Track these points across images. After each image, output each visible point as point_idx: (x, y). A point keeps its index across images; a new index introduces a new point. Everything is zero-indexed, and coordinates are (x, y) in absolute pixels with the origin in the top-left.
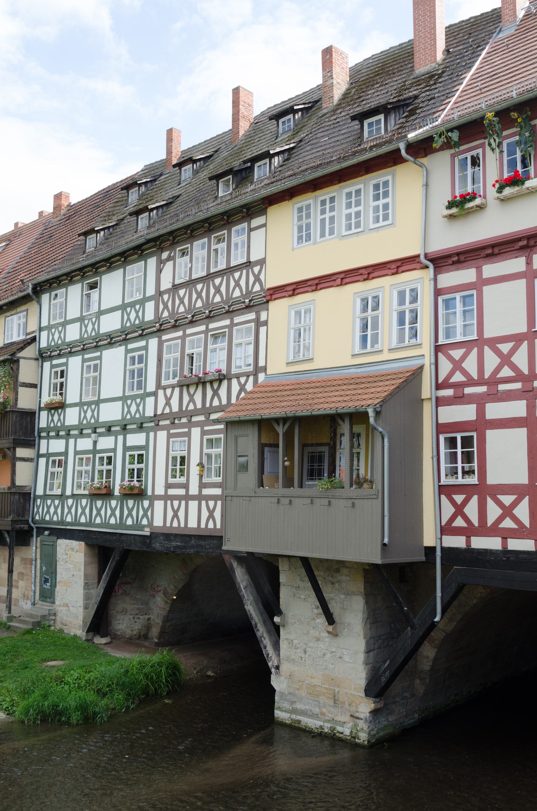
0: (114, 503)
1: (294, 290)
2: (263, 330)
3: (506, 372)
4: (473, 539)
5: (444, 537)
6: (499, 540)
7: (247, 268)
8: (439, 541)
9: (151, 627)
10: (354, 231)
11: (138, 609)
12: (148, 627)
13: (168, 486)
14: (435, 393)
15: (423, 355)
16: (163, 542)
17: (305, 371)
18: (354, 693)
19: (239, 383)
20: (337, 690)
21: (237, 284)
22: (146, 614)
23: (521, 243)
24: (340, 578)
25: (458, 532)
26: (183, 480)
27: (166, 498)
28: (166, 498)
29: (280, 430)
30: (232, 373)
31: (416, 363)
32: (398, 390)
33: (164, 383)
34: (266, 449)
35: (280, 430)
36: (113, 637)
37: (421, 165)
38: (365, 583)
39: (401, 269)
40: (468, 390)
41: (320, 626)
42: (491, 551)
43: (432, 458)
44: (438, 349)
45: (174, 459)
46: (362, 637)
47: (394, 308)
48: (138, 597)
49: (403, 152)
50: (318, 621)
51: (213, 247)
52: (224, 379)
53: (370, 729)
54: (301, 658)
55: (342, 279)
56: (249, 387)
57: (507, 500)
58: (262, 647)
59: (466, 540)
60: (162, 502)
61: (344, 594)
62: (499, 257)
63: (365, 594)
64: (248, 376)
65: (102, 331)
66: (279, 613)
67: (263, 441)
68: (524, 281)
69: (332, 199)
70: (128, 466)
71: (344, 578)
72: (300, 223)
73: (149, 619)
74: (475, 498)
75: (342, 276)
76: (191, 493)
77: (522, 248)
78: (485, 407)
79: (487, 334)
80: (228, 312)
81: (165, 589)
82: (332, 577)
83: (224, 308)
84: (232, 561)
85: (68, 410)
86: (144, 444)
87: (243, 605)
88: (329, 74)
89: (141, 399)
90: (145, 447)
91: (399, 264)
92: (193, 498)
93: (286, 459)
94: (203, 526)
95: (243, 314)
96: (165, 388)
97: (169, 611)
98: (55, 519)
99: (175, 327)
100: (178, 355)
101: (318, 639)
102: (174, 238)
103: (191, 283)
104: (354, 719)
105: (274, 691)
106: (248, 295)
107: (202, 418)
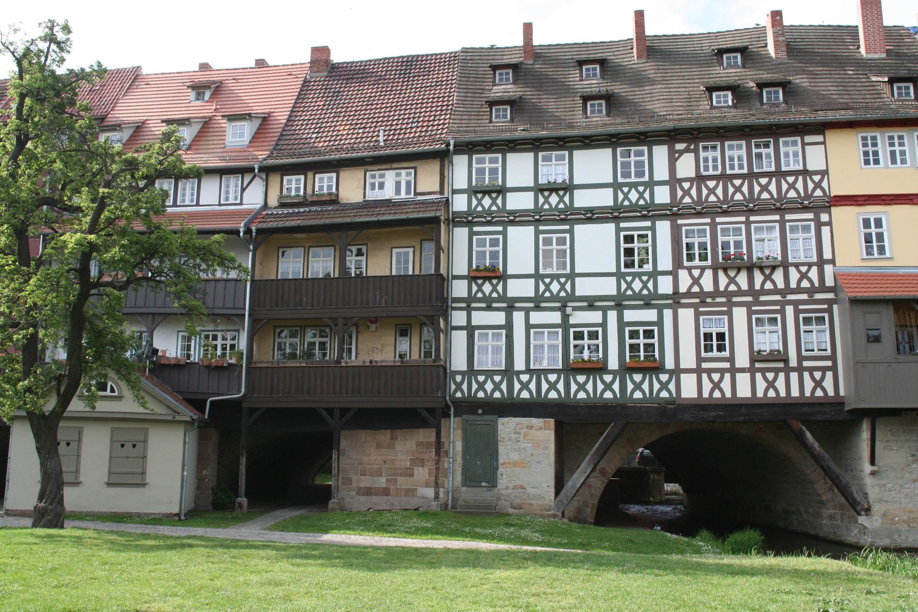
0: (608, 378)
2: (825, 230)
13: (700, 360)
19: (799, 271)
21: (792, 186)
26: (726, 354)
27: (698, 371)
33: (686, 263)
45: (708, 336)
50: (914, 466)
51: (754, 151)
52: (779, 266)
56: (814, 274)
60: (694, 376)
65: (577, 204)
69: (901, 138)
70: (628, 341)
76: (737, 366)
85: (509, 281)
90: (660, 323)
92: (742, 370)
94: (760, 394)
96: (689, 269)
98: (497, 395)
99: (699, 214)
100: (708, 240)
103: (725, 178)
107: (750, 299)
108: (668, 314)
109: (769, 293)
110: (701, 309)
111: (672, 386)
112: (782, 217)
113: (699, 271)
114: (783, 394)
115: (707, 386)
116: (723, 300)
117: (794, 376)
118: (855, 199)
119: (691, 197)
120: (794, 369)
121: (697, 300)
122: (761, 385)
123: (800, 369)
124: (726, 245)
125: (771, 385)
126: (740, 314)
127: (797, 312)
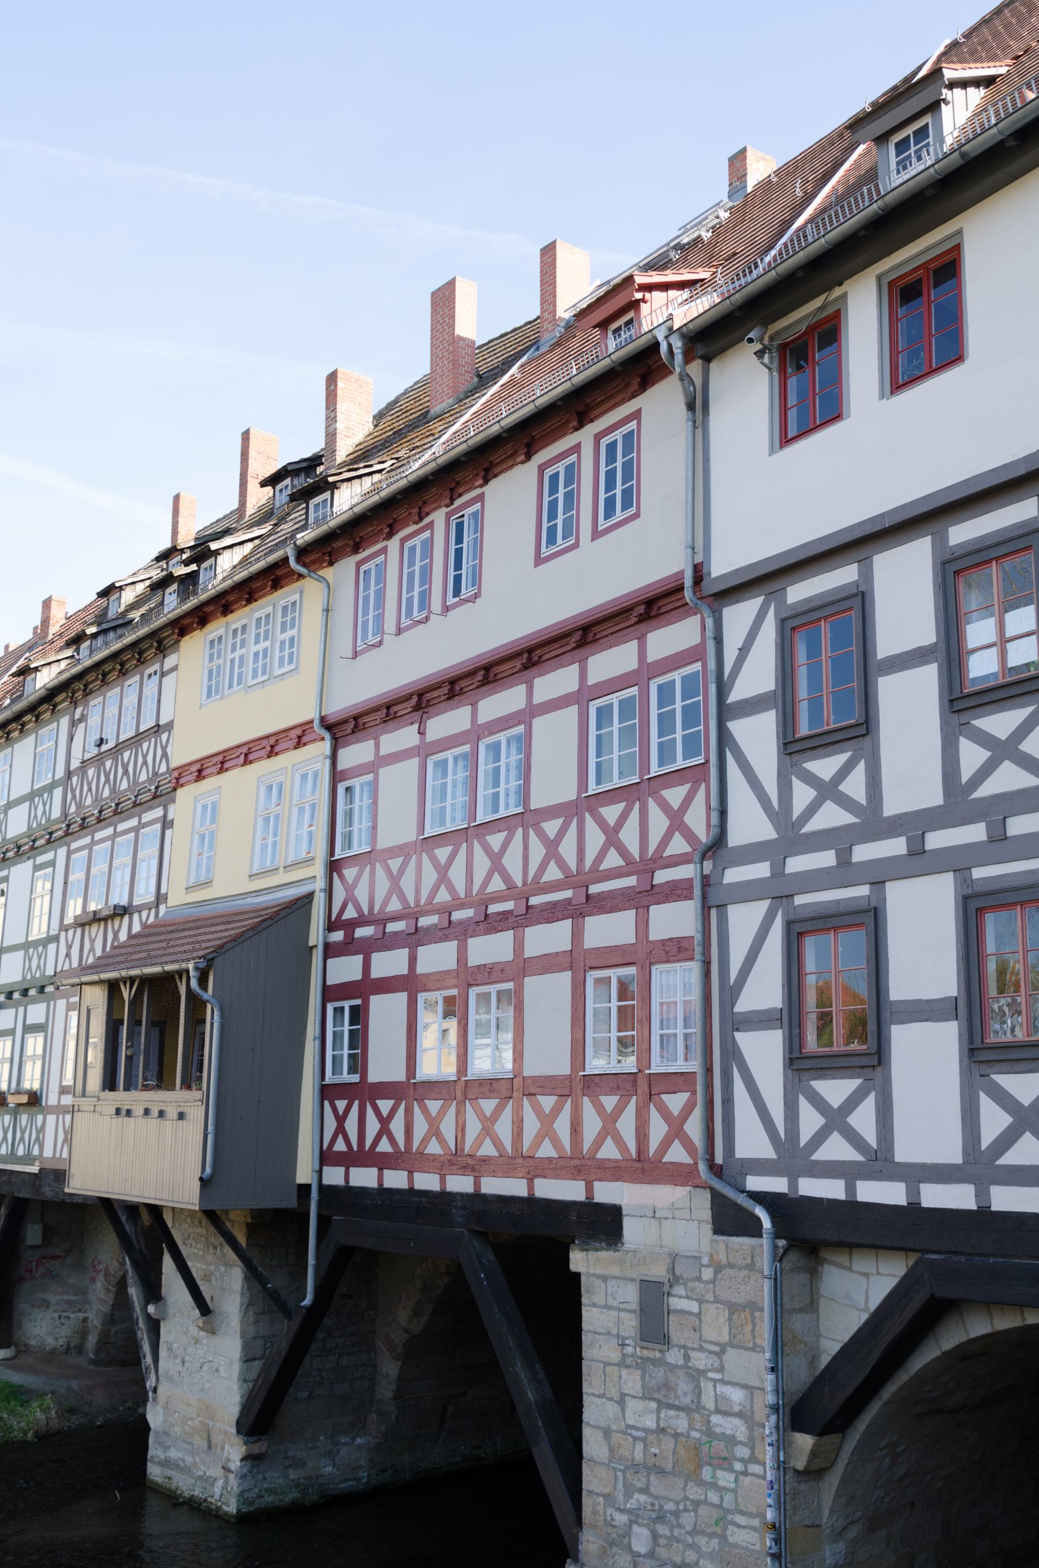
1: (200, 771)
2: (168, 832)
4: (353, 1170)
5: (325, 1169)
6: (374, 1171)
8: (316, 1176)
9: (88, 1332)
11: (67, 1302)
12: (83, 1334)
13: (63, 1091)
14: (325, 937)
20: (211, 1424)
22: (80, 1311)
27: (59, 1110)
28: (59, 1110)
32: (252, 933)
36: (23, 1349)
40: (361, 932)
44: (334, 867)
46: (238, 1336)
47: (295, 803)
48: (71, 1281)
52: (125, 914)
53: (241, 1489)
55: (246, 755)
57: (385, 1106)
58: (142, 1356)
69: (244, 627)
73: (85, 1320)
77: (417, 708)
80: (135, 805)
81: (107, 1267)
83: (130, 799)
86: (43, 1021)
88: (332, 414)
101: (197, 1341)
102: (86, 686)
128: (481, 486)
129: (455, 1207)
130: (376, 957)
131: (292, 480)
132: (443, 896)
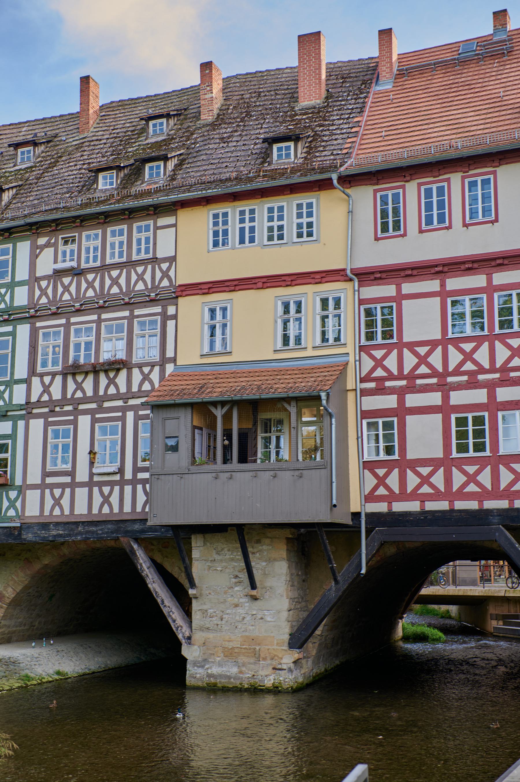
3: (423, 370)
6: (418, 503)
7: (153, 263)
8: (363, 507)
10: (276, 241)
13: (45, 474)
15: (348, 354)
16: (39, 532)
17: (222, 363)
18: (277, 647)
19: (142, 372)
20: (258, 648)
21: (141, 277)
23: (437, 269)
24: (260, 548)
25: (381, 499)
26: (68, 467)
27: (42, 487)
29: (219, 413)
30: (133, 362)
31: (344, 359)
33: (39, 369)
34: (196, 430)
35: (219, 413)
37: (348, 196)
38: (287, 550)
39: (324, 280)
40: (388, 384)
41: (238, 593)
42: (410, 512)
43: (358, 439)
44: (362, 348)
47: (317, 312)
49: (335, 182)
50: (236, 589)
52: (122, 369)
54: (217, 625)
56: (155, 376)
57: (425, 471)
58: (170, 621)
59: (388, 506)
61: (266, 561)
62: (416, 278)
63: (287, 560)
64: (153, 366)
66: (193, 585)
67: (195, 423)
68: (438, 299)
69: (252, 212)
71: (265, 547)
72: (216, 228)
74: (396, 471)
75: (264, 280)
76: (77, 480)
78: (405, 397)
79: (406, 339)
82: (253, 547)
84: (132, 543)
87: (146, 585)
88: (208, 88)
89: (7, 386)
90: (13, 436)
91: (324, 275)
92: (82, 485)
93: (225, 438)
94: (95, 511)
95: (145, 307)
96: (41, 376)
97: (3, 616)
99: (55, 315)
101: (236, 606)
104: (278, 672)
105: (185, 660)
106: (154, 290)
107: (94, 406)
108: (21, 424)
109: (112, 398)
110: (50, 419)
111: (18, 504)
112: (132, 312)
113: (50, 377)
114: (116, 510)
115: (49, 502)
116: (70, 408)
117: (128, 489)
118: (200, 287)
119: (47, 297)
120: (128, 482)
121: (46, 410)
122: (97, 499)
123: (134, 482)
124: (78, 346)
125: (106, 500)
126: (84, 421)
127: (137, 418)
128: (494, 167)
129: (491, 516)
130: (408, 396)
131: (168, 121)
132: (469, 366)
